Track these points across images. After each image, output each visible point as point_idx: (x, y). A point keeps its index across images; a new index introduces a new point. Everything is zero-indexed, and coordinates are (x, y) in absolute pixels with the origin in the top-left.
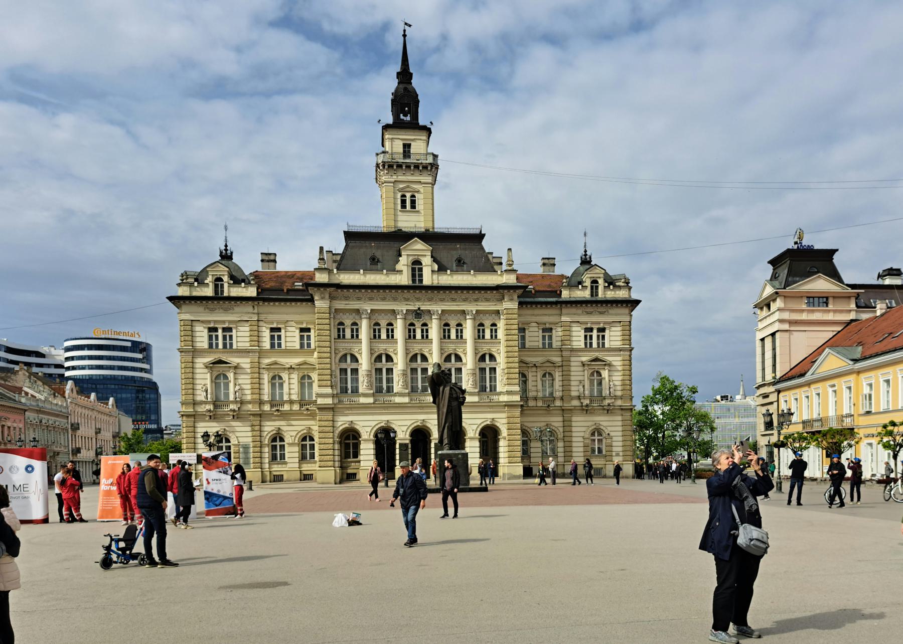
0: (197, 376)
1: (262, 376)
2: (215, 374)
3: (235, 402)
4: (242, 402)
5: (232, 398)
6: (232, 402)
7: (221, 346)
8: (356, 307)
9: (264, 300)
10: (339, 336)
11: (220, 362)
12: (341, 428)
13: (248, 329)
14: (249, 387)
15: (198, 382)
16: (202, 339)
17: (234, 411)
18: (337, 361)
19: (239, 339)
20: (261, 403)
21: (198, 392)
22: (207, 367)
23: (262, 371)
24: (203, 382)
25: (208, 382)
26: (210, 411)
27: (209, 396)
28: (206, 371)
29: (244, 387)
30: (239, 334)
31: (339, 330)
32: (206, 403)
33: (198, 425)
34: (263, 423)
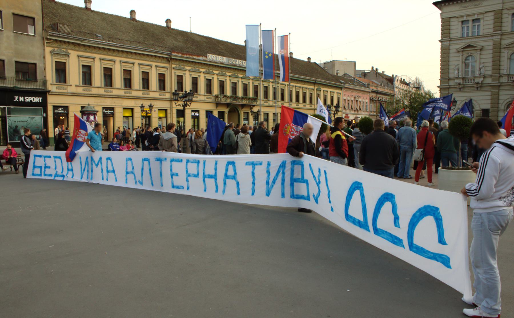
0: (451, 59)
1: (502, 55)
2: (465, 56)
3: (480, 77)
4: (484, 77)
5: (477, 73)
6: (477, 77)
7: (470, 35)
11: (469, 46)
13: (492, 18)
14: (491, 64)
15: (451, 63)
16: (456, 30)
17: (478, 83)
19: (485, 27)
20: (501, 76)
21: (451, 71)
22: (459, 52)
23: (503, 50)
24: (456, 63)
25: (460, 63)
26: (459, 84)
27: (460, 74)
29: (486, 65)
30: (485, 23)
32: (457, 78)
34: (501, 93)
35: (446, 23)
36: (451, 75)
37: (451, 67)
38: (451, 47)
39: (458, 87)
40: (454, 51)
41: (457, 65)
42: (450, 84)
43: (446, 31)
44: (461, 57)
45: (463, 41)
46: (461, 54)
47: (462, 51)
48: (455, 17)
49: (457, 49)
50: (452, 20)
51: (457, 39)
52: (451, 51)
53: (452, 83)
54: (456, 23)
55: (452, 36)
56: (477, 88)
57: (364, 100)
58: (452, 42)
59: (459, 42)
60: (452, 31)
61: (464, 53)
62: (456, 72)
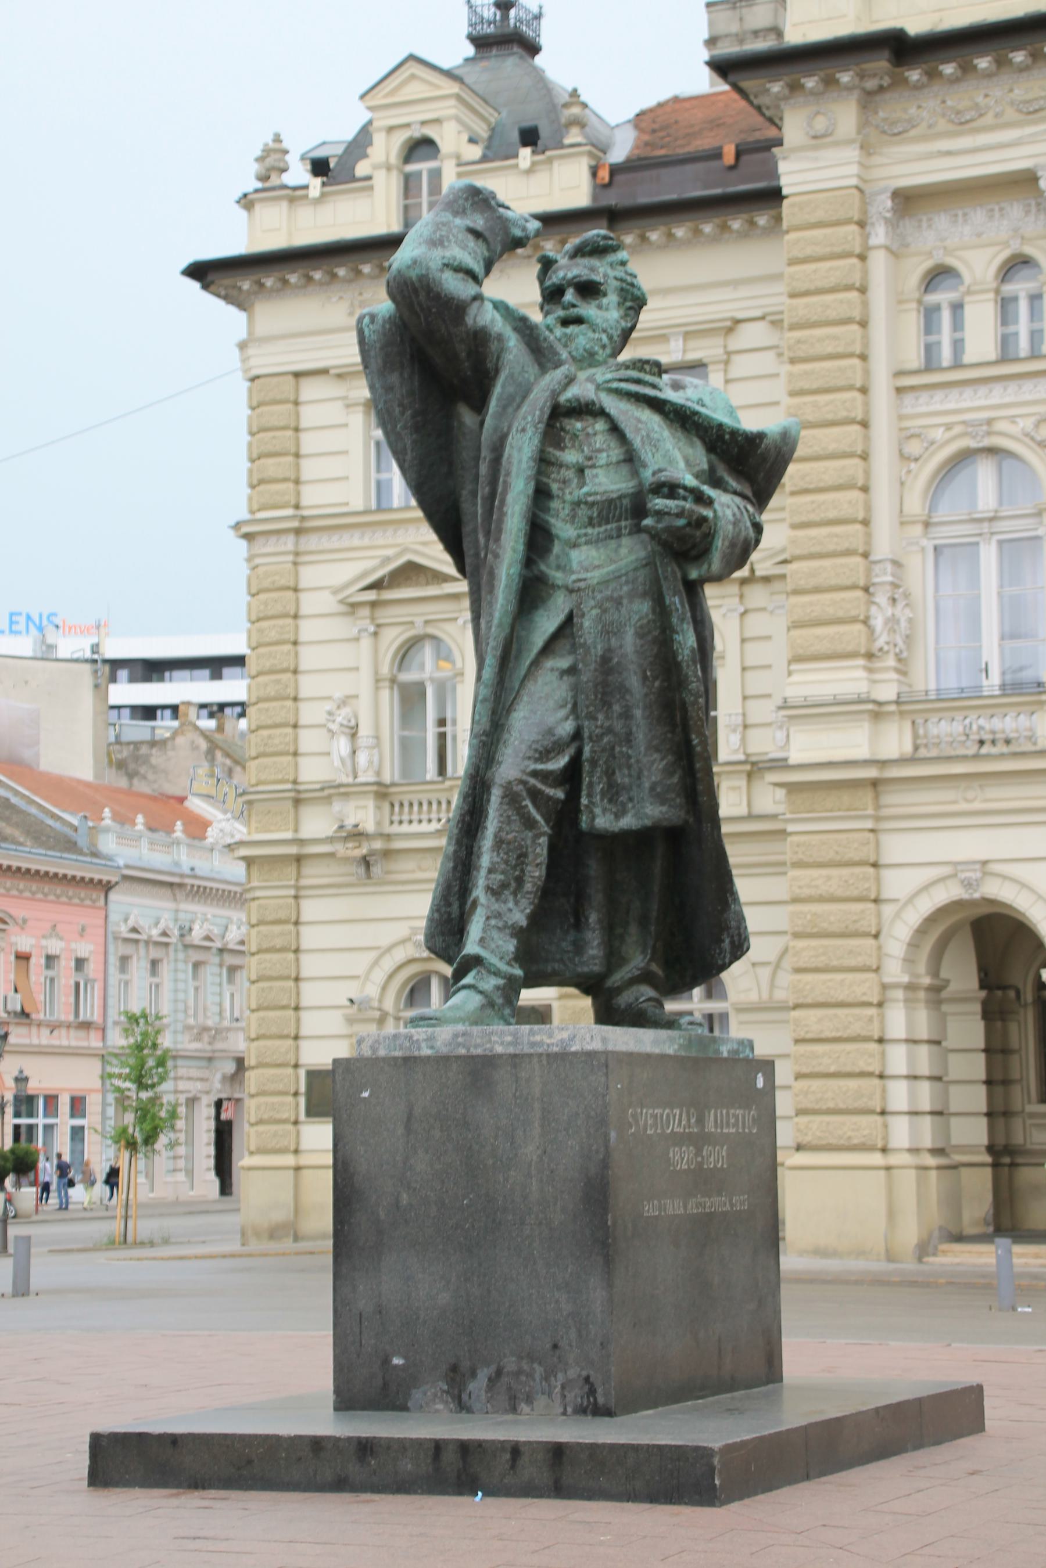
0: (308, 658)
2: (393, 638)
8: (1014, 161)
9: (613, 217)
10: (930, 364)
12: (926, 906)
15: (307, 686)
18: (915, 505)
21: (308, 740)
24: (338, 686)
25: (363, 684)
26: (357, 835)
27: (362, 758)
28: (344, 627)
31: (930, 314)
33: (310, 909)
35: (278, 414)
36: (312, 772)
37: (309, 713)
38: (308, 576)
39: (340, 849)
40: (327, 602)
41: (344, 702)
42: (305, 833)
43: (272, 467)
44: (366, 643)
45: (380, 538)
46: (363, 621)
47: (374, 604)
48: (323, 372)
49: (336, 591)
50: (310, 389)
51: (341, 523)
52: (310, 603)
53: (317, 824)
54: (334, 413)
55: (313, 497)
56: (366, 862)
57: (54, 946)
58: (311, 542)
59: (355, 539)
60: (309, 469)
61: (385, 615)
62: (342, 745)
